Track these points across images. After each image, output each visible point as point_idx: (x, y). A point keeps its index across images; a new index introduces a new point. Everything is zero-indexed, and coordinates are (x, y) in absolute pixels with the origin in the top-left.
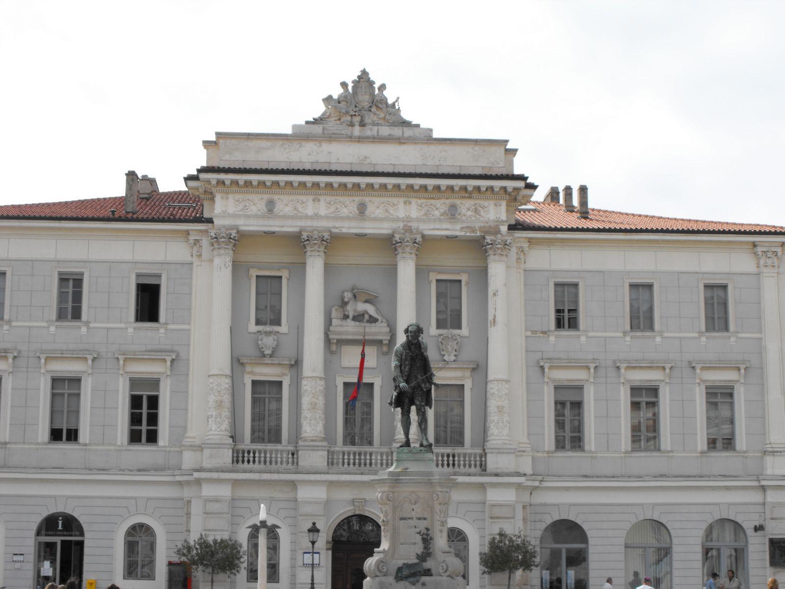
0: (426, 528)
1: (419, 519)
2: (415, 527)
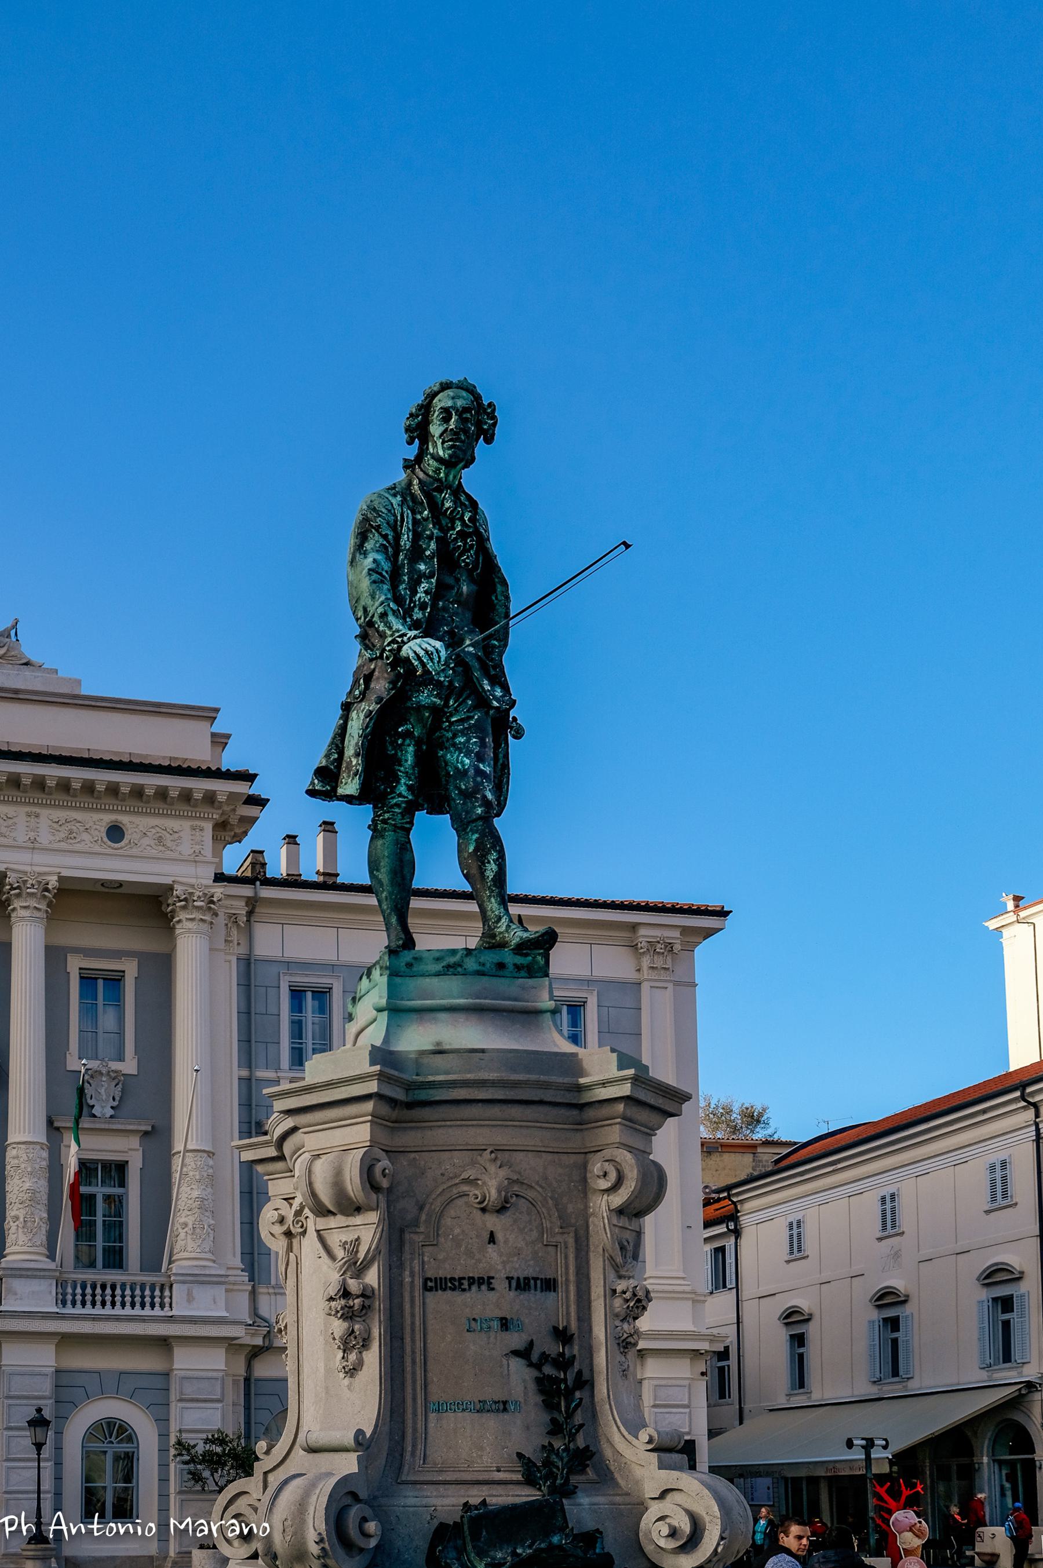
0: (555, 1329)
1: (522, 1285)
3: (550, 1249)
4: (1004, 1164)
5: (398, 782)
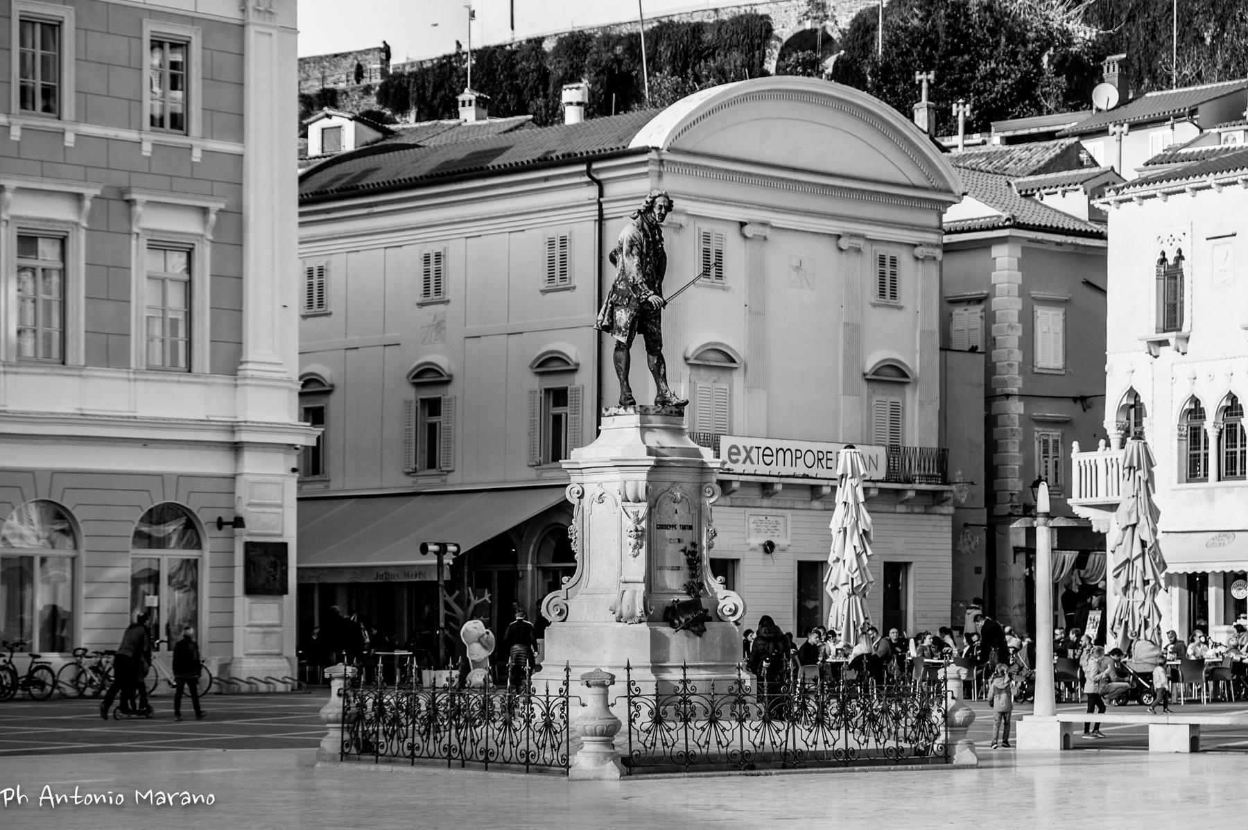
1: (684, 528)
2: (679, 541)
4: (564, 241)
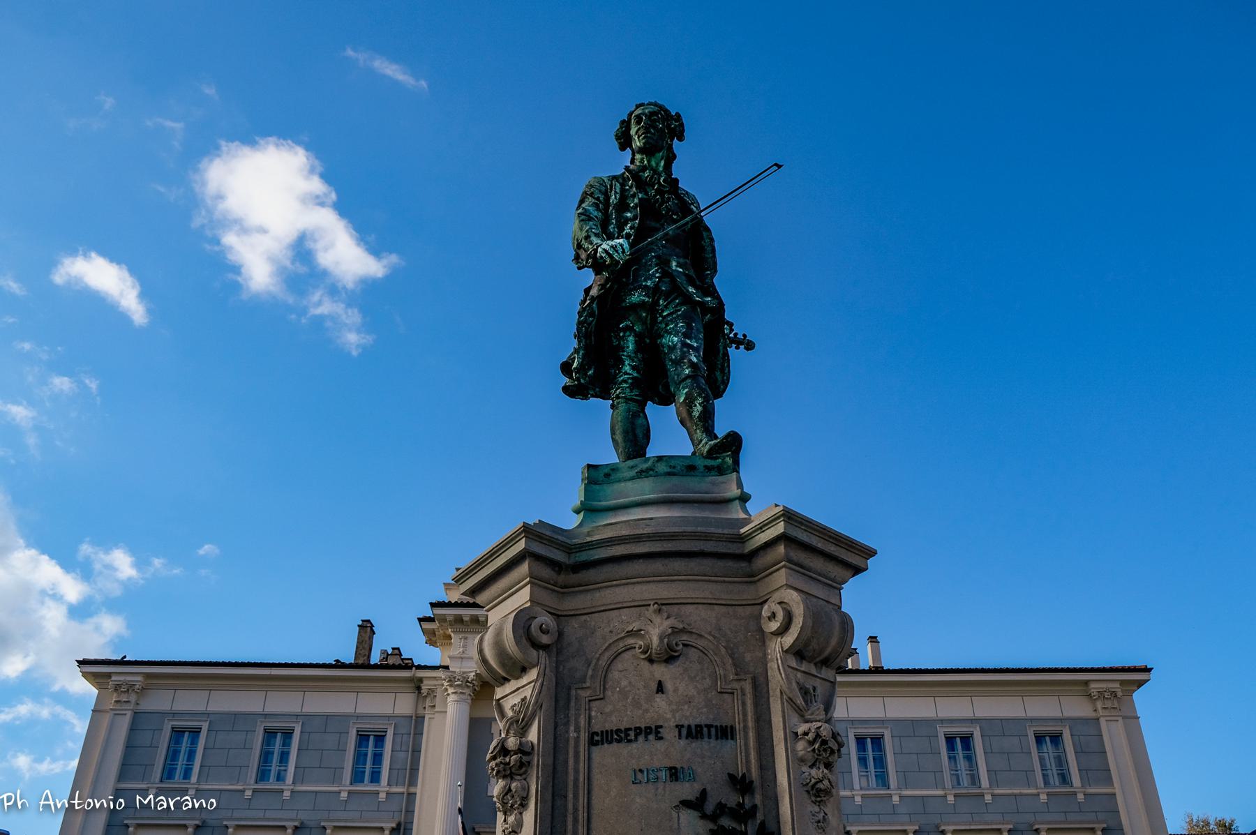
0: (732, 777)
1: (694, 733)
3: (726, 696)
5: (623, 364)
